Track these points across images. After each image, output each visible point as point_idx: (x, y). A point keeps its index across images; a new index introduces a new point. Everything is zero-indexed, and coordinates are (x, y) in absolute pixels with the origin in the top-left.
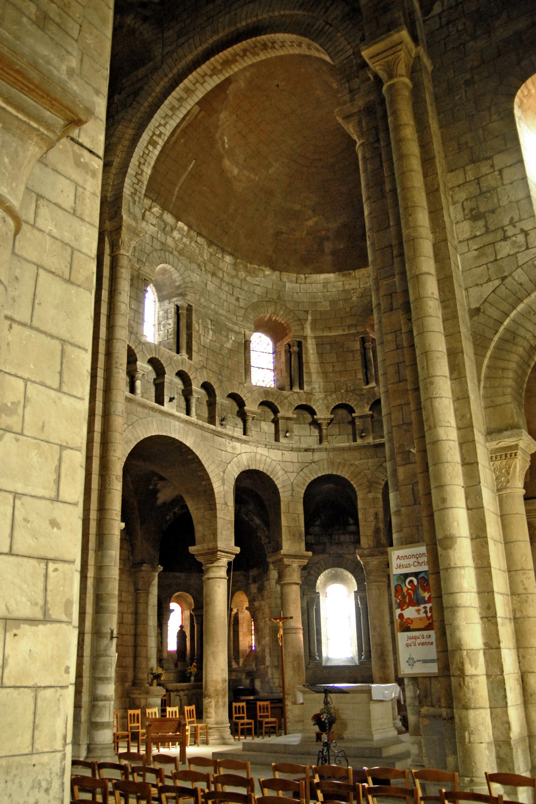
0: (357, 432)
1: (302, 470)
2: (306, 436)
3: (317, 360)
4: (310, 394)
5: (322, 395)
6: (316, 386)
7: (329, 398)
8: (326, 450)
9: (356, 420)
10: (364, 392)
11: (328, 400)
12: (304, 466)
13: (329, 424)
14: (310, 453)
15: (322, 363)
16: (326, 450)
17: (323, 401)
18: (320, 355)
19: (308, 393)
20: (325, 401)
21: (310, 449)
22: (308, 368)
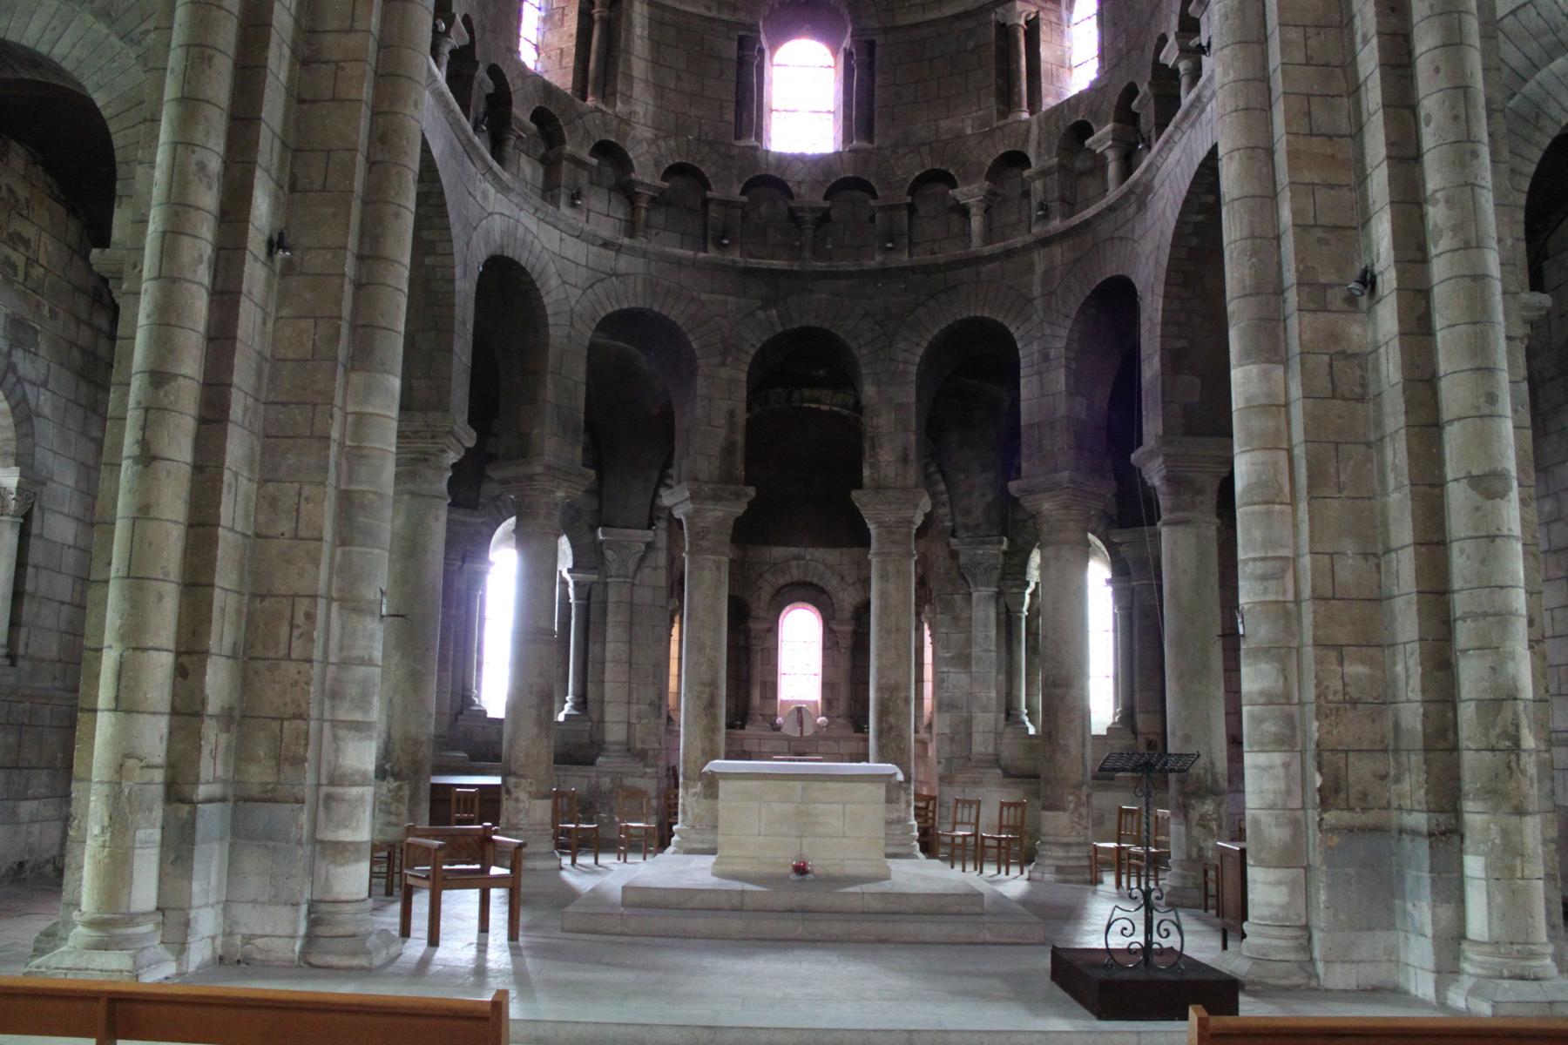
0: (710, 233)
1: (591, 286)
2: (603, 214)
3: (646, 54)
4: (625, 121)
5: (649, 134)
6: (640, 110)
7: (661, 143)
8: (644, 254)
9: (712, 207)
10: (735, 152)
11: (658, 147)
12: (601, 276)
13: (653, 199)
14: (612, 254)
15: (656, 62)
16: (644, 254)
17: (650, 145)
18: (656, 44)
19: (622, 120)
20: (654, 148)
21: (613, 244)
22: (628, 63)
